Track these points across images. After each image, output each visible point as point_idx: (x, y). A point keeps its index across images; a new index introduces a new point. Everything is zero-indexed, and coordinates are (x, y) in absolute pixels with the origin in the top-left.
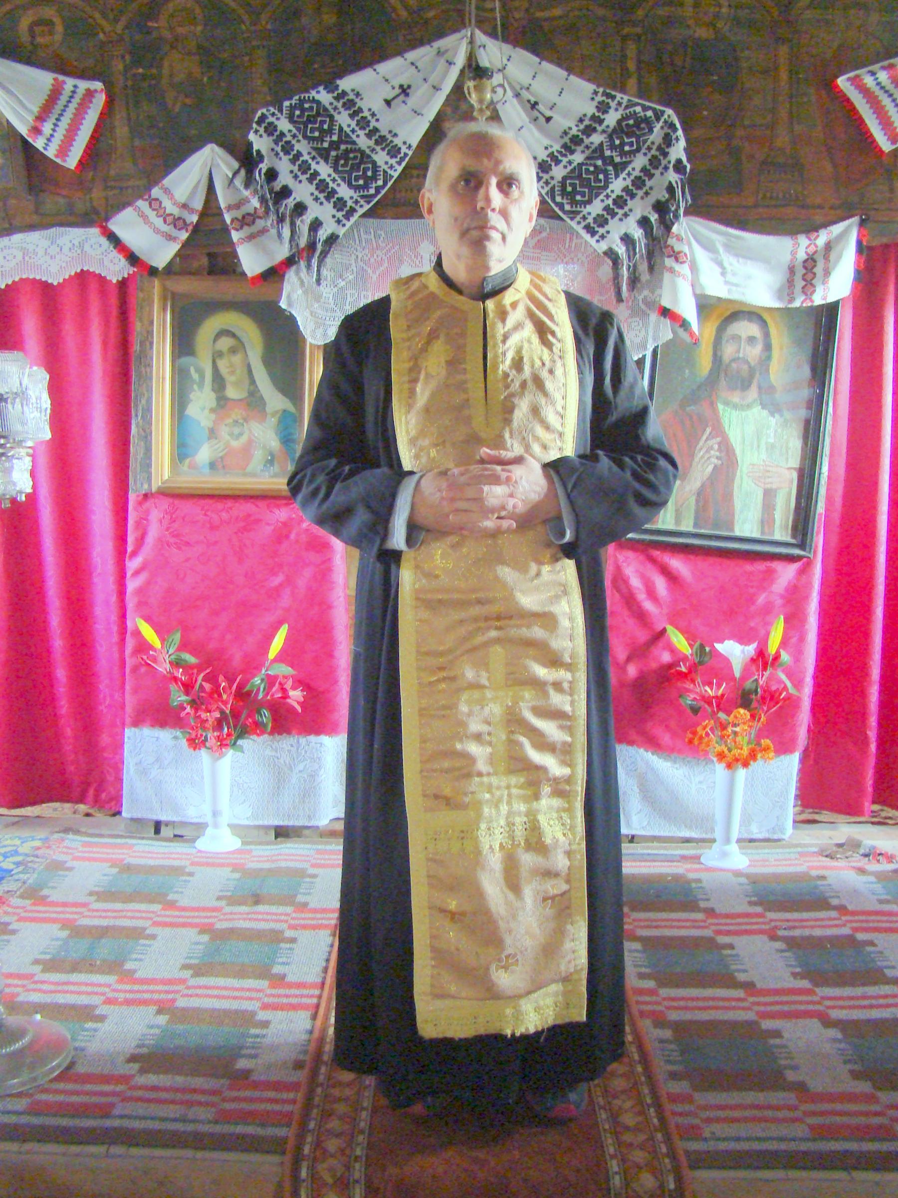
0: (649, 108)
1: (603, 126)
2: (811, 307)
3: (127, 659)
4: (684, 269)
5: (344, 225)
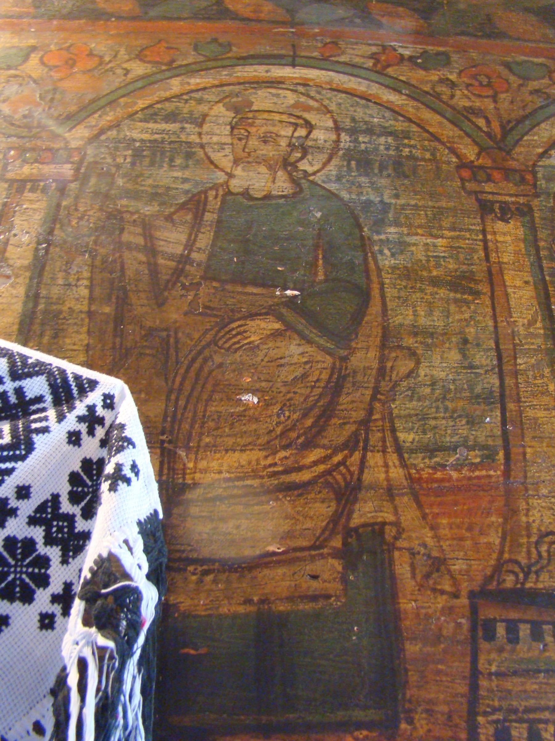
0: (39, 369)
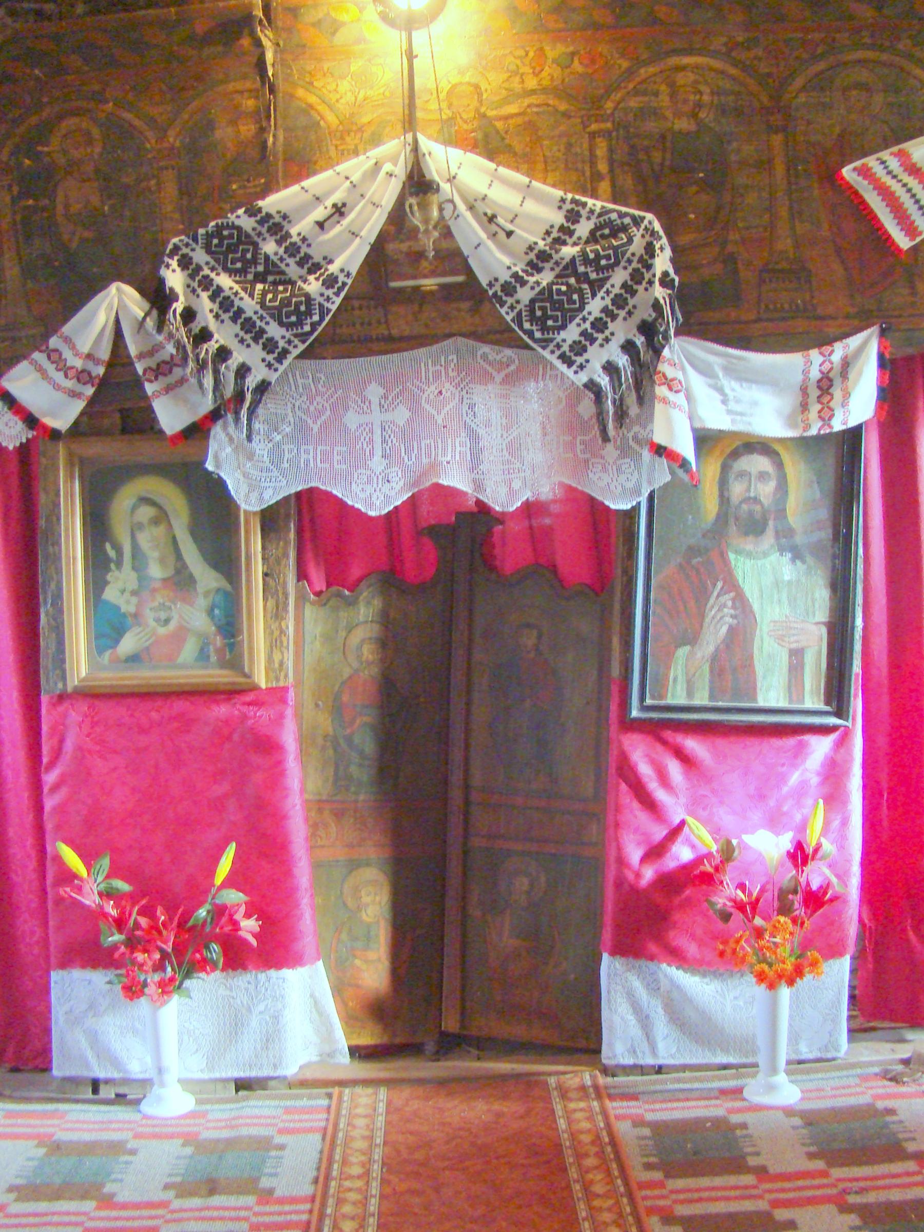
1: (575, 238)
2: (830, 434)
3: (49, 889)
4: (680, 399)
5: (276, 370)
